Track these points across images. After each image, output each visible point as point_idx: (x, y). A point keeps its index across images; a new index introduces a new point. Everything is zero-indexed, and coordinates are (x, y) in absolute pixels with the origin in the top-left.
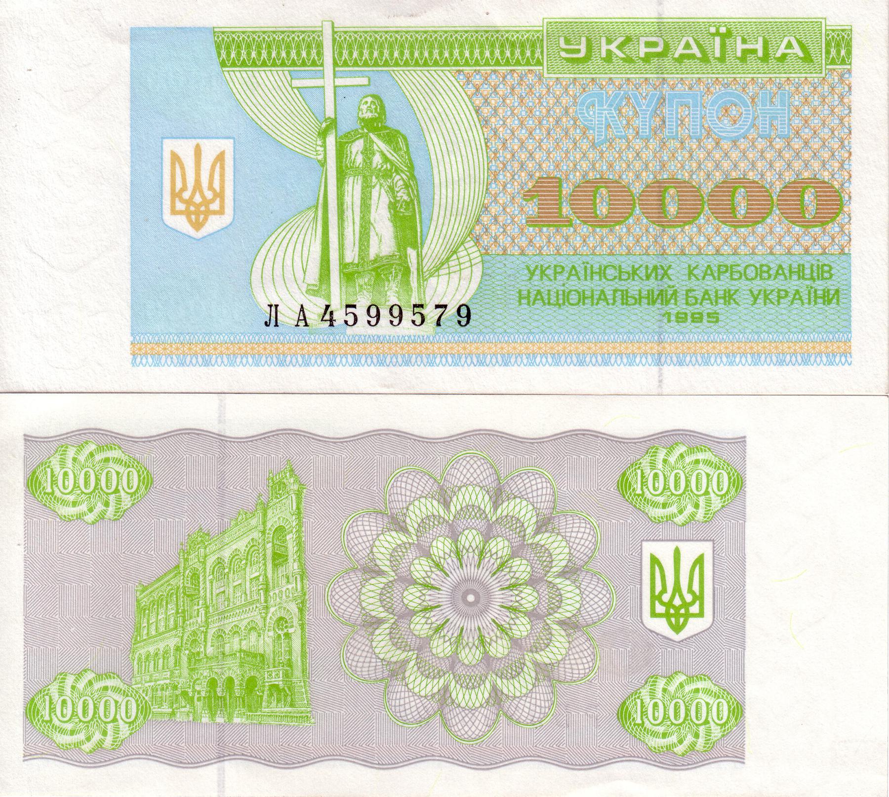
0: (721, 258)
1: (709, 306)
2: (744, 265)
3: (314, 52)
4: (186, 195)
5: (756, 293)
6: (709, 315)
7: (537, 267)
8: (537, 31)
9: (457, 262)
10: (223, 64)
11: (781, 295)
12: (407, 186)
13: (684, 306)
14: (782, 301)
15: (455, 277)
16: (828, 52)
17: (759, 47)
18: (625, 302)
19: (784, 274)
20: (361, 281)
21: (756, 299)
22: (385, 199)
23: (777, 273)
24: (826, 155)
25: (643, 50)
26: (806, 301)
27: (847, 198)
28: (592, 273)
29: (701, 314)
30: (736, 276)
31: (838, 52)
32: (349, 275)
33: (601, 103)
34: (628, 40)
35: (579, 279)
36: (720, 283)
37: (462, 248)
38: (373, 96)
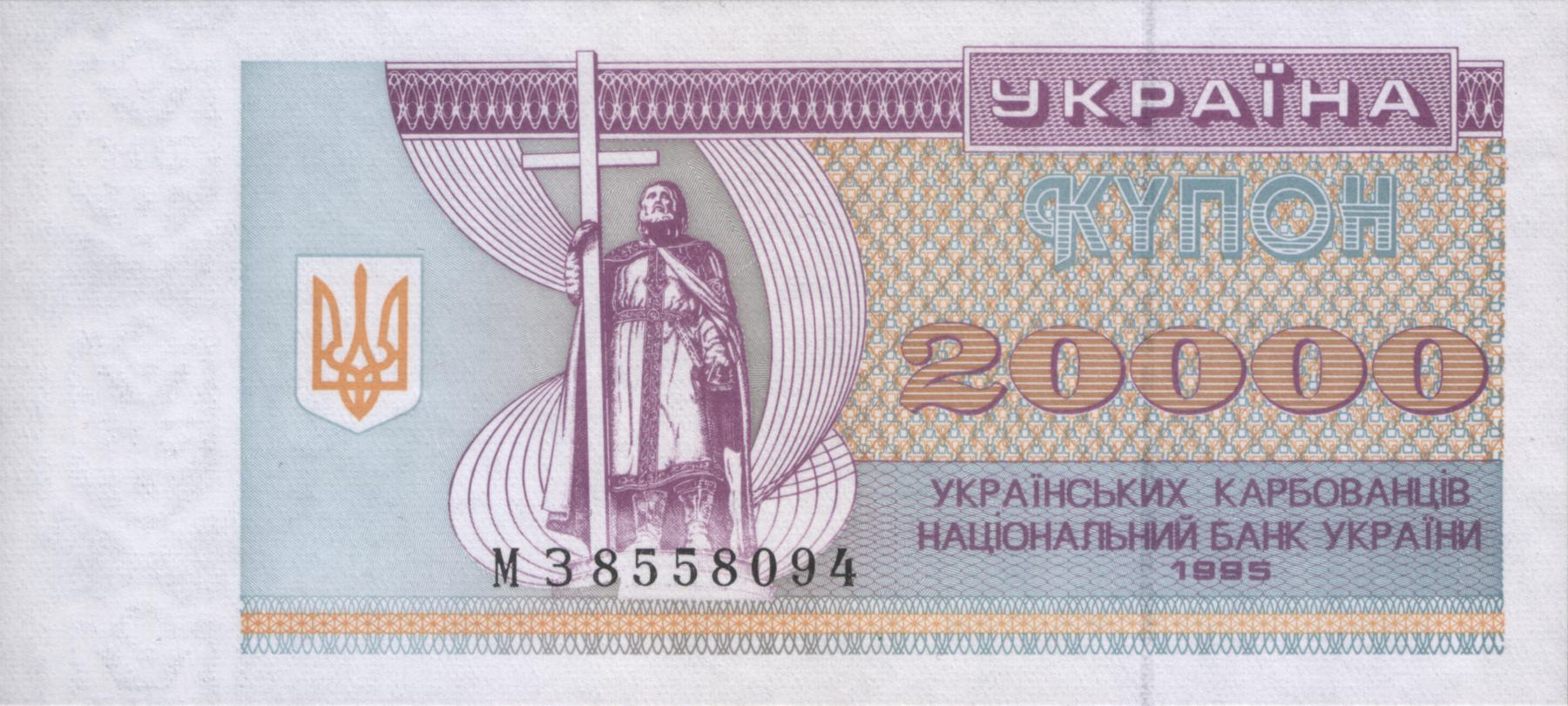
0: (1273, 468)
1: (1253, 550)
2: (1314, 480)
3: (562, 107)
4: (340, 355)
5: (1334, 528)
6: (1252, 566)
7: (950, 484)
8: (954, 70)
9: (810, 474)
10: (402, 128)
11: (1380, 531)
12: (723, 339)
13: (1210, 551)
14: (1380, 542)
15: (807, 499)
16: (1462, 108)
17: (1342, 98)
18: (1105, 543)
19: (1383, 495)
20: (643, 507)
21: (1334, 538)
22: (686, 363)
23: (1372, 495)
24: (1460, 288)
25: (1138, 105)
26: (1422, 542)
27: (1496, 361)
28: (1048, 493)
29: (1239, 565)
30: (1300, 498)
31: (1480, 108)
32: (622, 495)
33: (1065, 198)
34: (1112, 86)
35: (1025, 503)
36: (1272, 510)
37: (820, 449)
38: (663, 183)
